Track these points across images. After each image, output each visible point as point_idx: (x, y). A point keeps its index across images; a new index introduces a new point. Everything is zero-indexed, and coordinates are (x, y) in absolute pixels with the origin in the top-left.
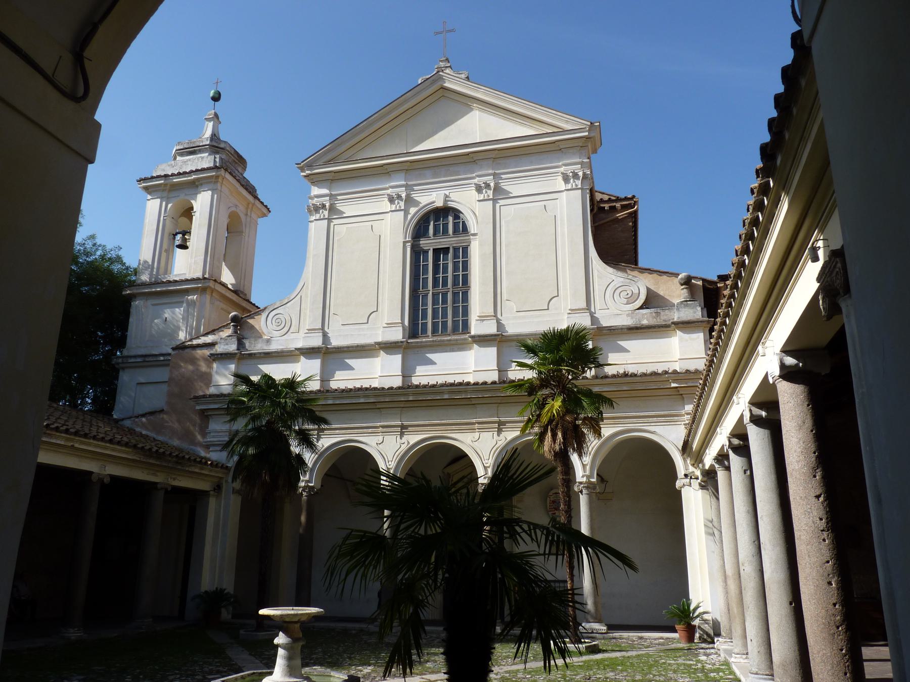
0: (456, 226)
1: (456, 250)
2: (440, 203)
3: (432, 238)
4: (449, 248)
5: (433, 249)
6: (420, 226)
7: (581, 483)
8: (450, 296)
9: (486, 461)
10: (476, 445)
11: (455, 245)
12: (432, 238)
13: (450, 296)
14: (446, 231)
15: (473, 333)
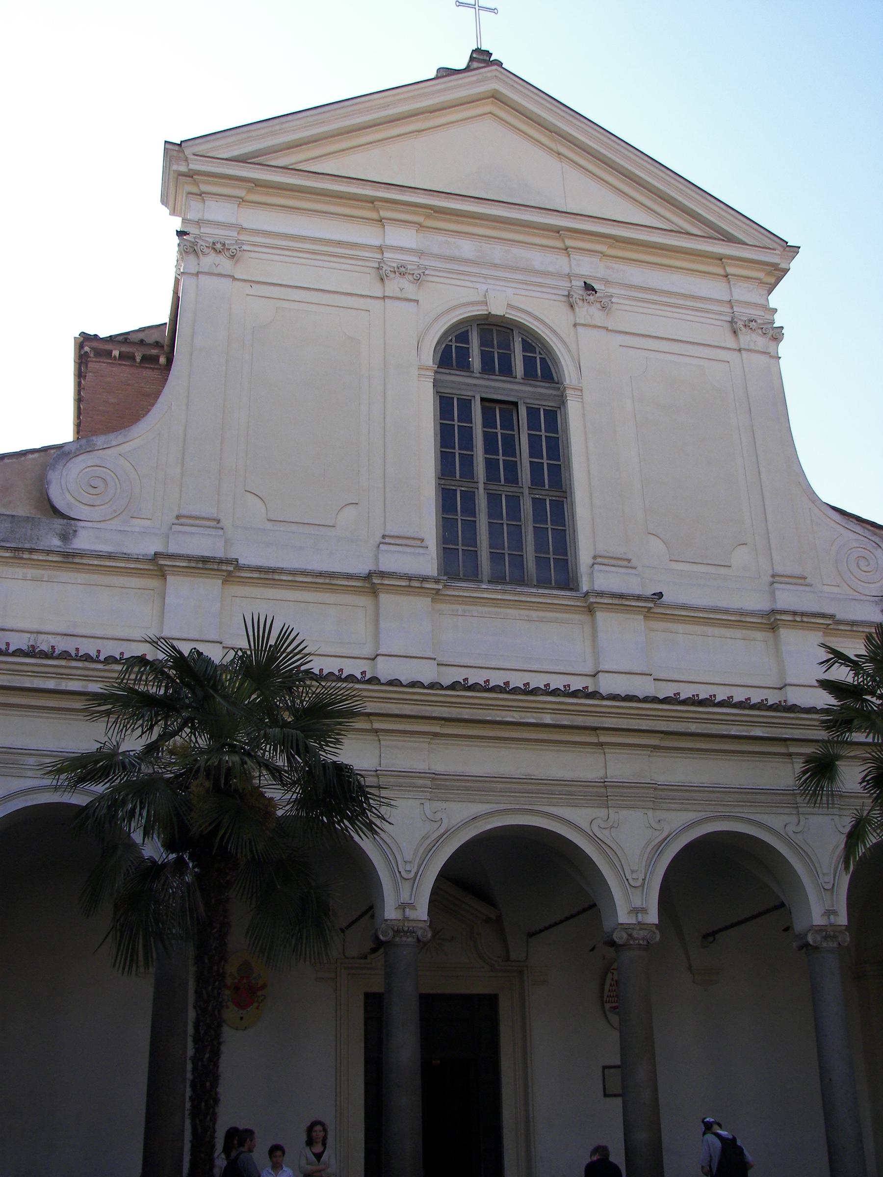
0: (529, 363)
1: (533, 413)
2: (498, 309)
3: (478, 375)
4: (515, 404)
5: (483, 400)
6: (448, 348)
7: (820, 929)
8: (527, 506)
9: (635, 876)
10: (604, 835)
11: (528, 401)
12: (478, 375)
13: (527, 506)
14: (507, 370)
15: (585, 587)
